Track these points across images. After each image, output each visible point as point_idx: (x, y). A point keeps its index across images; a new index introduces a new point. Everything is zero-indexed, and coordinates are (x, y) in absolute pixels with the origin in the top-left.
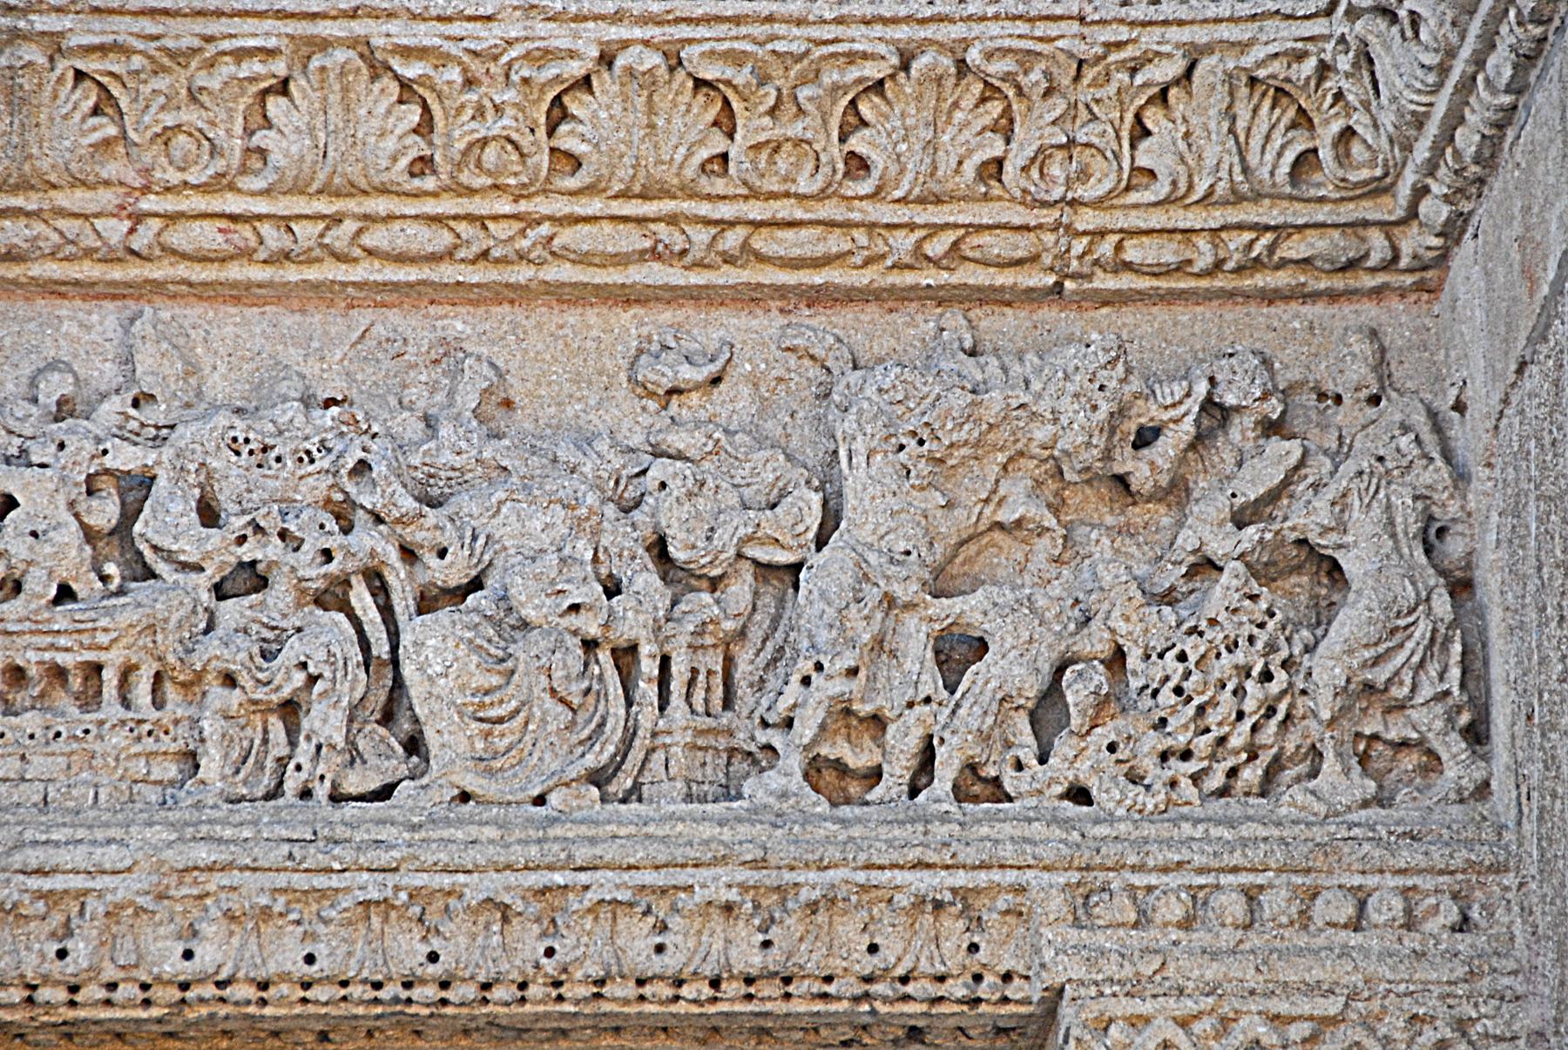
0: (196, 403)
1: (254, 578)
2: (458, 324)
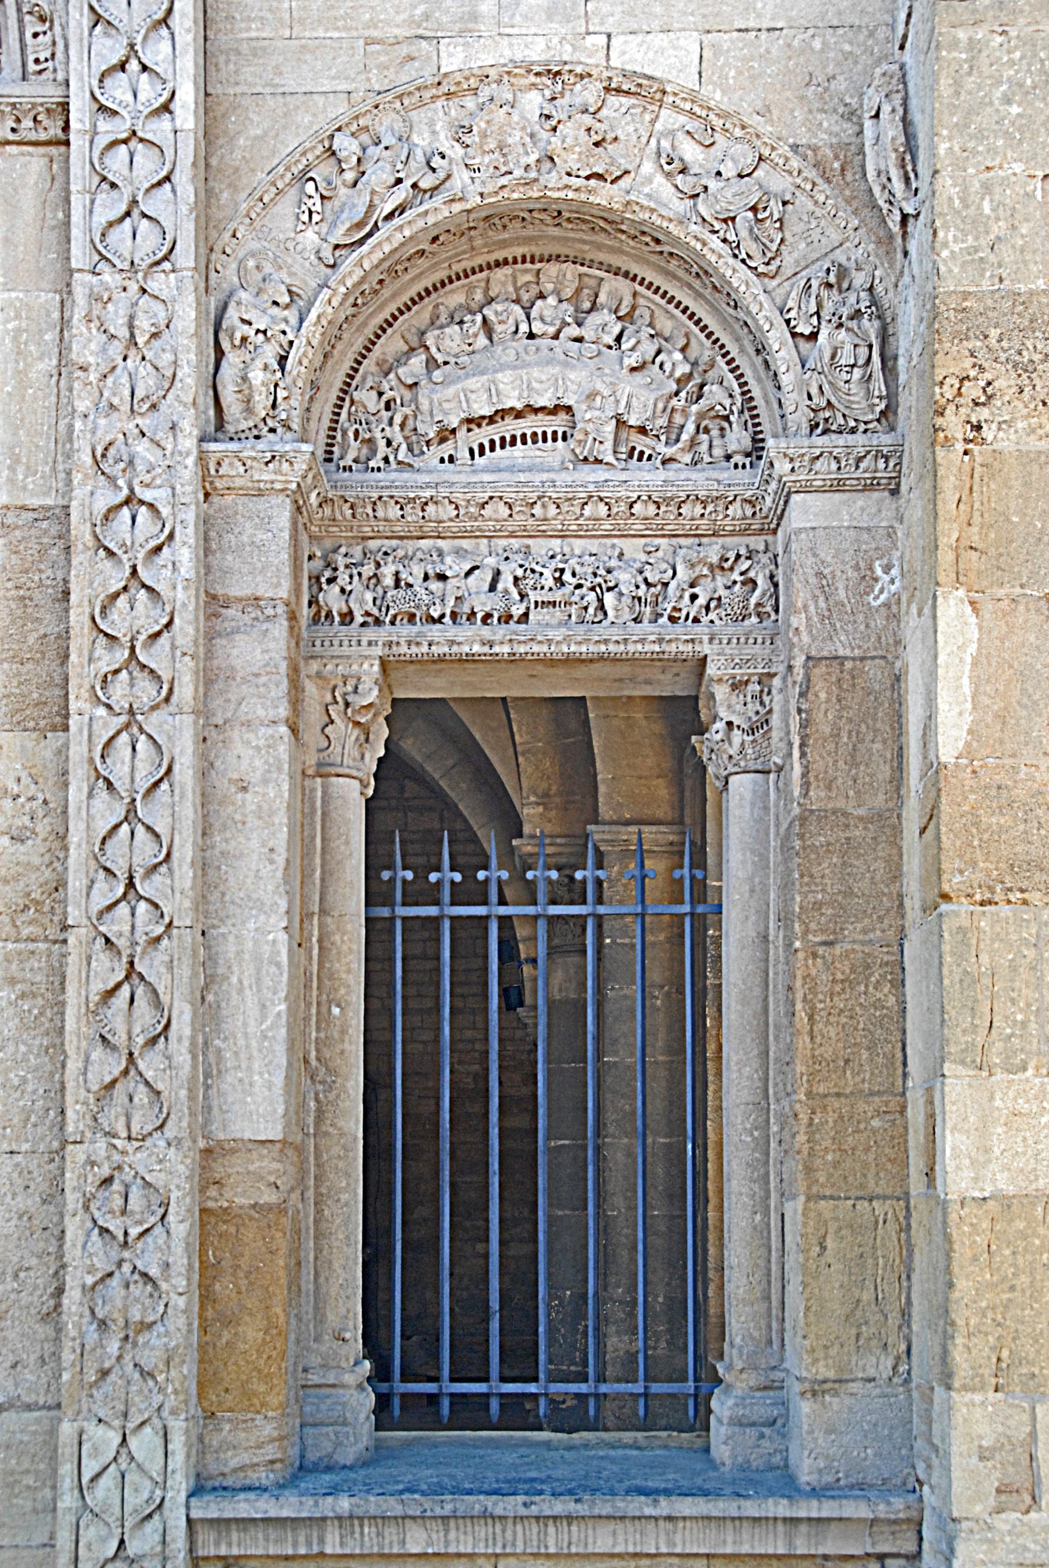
0: (573, 555)
1: (579, 586)
2: (615, 541)
